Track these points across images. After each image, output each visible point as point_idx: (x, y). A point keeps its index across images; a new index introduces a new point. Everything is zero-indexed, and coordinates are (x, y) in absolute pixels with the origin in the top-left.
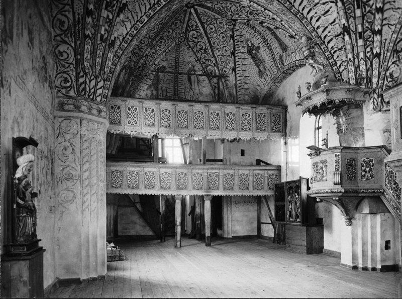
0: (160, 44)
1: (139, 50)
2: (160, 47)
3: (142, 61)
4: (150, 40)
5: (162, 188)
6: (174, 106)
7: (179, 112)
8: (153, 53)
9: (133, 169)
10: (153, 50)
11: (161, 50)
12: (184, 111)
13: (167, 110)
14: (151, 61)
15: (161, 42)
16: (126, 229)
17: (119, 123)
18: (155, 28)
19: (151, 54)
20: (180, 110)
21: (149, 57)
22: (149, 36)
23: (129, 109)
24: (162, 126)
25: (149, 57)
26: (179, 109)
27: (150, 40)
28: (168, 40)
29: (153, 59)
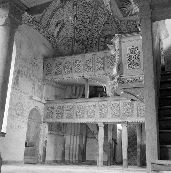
1: (85, 27)
2: (99, 22)
3: (89, 34)
4: (90, 19)
5: (88, 117)
6: (94, 55)
7: (98, 59)
8: (96, 27)
9: (70, 104)
10: (95, 25)
11: (100, 24)
12: (100, 57)
14: (96, 33)
15: (98, 19)
16: (92, 156)
17: (60, 74)
18: (90, 11)
19: (95, 28)
20: (98, 57)
21: (94, 31)
22: (88, 17)
23: (66, 64)
24: (86, 71)
25: (94, 31)
26: (97, 57)
27: (90, 19)
29: (97, 31)
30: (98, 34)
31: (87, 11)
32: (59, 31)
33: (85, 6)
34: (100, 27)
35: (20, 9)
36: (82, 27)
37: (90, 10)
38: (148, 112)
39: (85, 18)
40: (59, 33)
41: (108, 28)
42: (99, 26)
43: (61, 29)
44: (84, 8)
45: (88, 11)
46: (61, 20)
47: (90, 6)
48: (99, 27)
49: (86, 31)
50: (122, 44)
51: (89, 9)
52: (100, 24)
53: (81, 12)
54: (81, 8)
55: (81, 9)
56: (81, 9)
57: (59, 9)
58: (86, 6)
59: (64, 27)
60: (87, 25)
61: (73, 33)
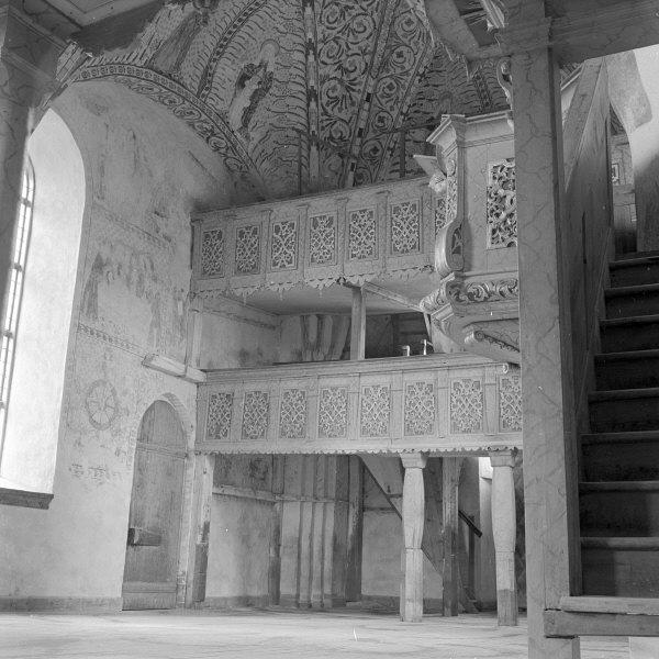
0: (400, 60)
1: (348, 89)
2: (403, 68)
3: (364, 114)
4: (368, 58)
5: (364, 431)
6: (382, 196)
7: (397, 209)
8: (390, 87)
9: (294, 384)
10: (389, 81)
11: (407, 73)
13: (364, 211)
14: (392, 108)
15: (400, 55)
16: (384, 578)
17: (255, 268)
18: (366, 24)
20: (398, 204)
21: (383, 101)
22: (360, 48)
23: (277, 230)
24: (353, 256)
25: (383, 101)
26: (394, 201)
27: (368, 58)
28: (416, 43)
29: (396, 102)
30: (402, 113)
31: (355, 26)
32: (247, 104)
33: (347, 7)
34: (407, 84)
35: (48, 33)
36: (339, 86)
37: (367, 21)
38: (534, 412)
39: (350, 53)
40: (248, 112)
41: (440, 88)
42: (402, 82)
43: (256, 97)
44: (342, 14)
45: (360, 24)
46: (257, 63)
47: (368, 5)
48: (403, 86)
49: (353, 104)
50: (469, 151)
51: (360, 18)
52: (407, 73)
53: (334, 32)
54: (334, 13)
55: (331, 19)
56: (331, 19)
57: (249, 23)
58: (353, 8)
59: (267, 89)
60: (355, 79)
61: (303, 114)
